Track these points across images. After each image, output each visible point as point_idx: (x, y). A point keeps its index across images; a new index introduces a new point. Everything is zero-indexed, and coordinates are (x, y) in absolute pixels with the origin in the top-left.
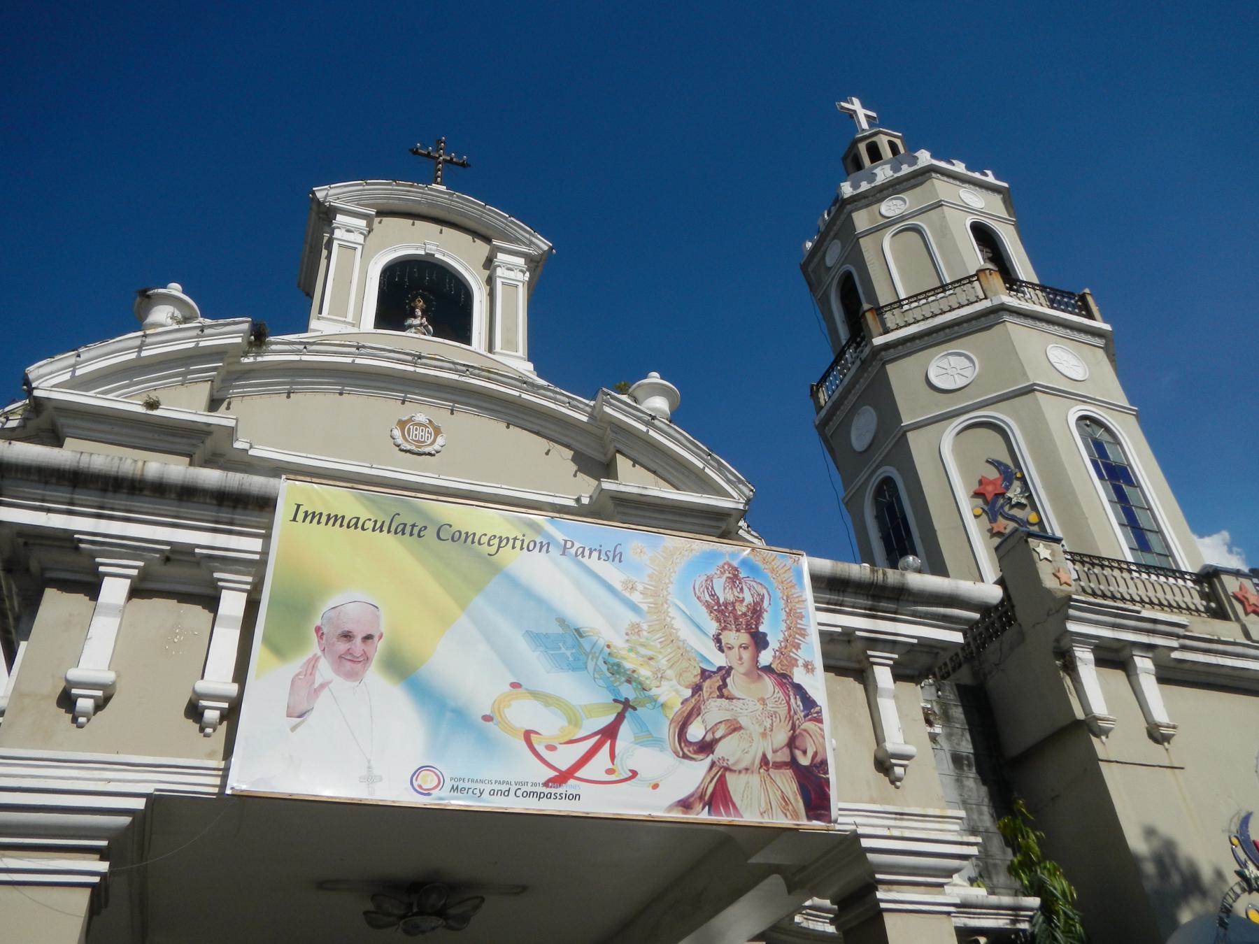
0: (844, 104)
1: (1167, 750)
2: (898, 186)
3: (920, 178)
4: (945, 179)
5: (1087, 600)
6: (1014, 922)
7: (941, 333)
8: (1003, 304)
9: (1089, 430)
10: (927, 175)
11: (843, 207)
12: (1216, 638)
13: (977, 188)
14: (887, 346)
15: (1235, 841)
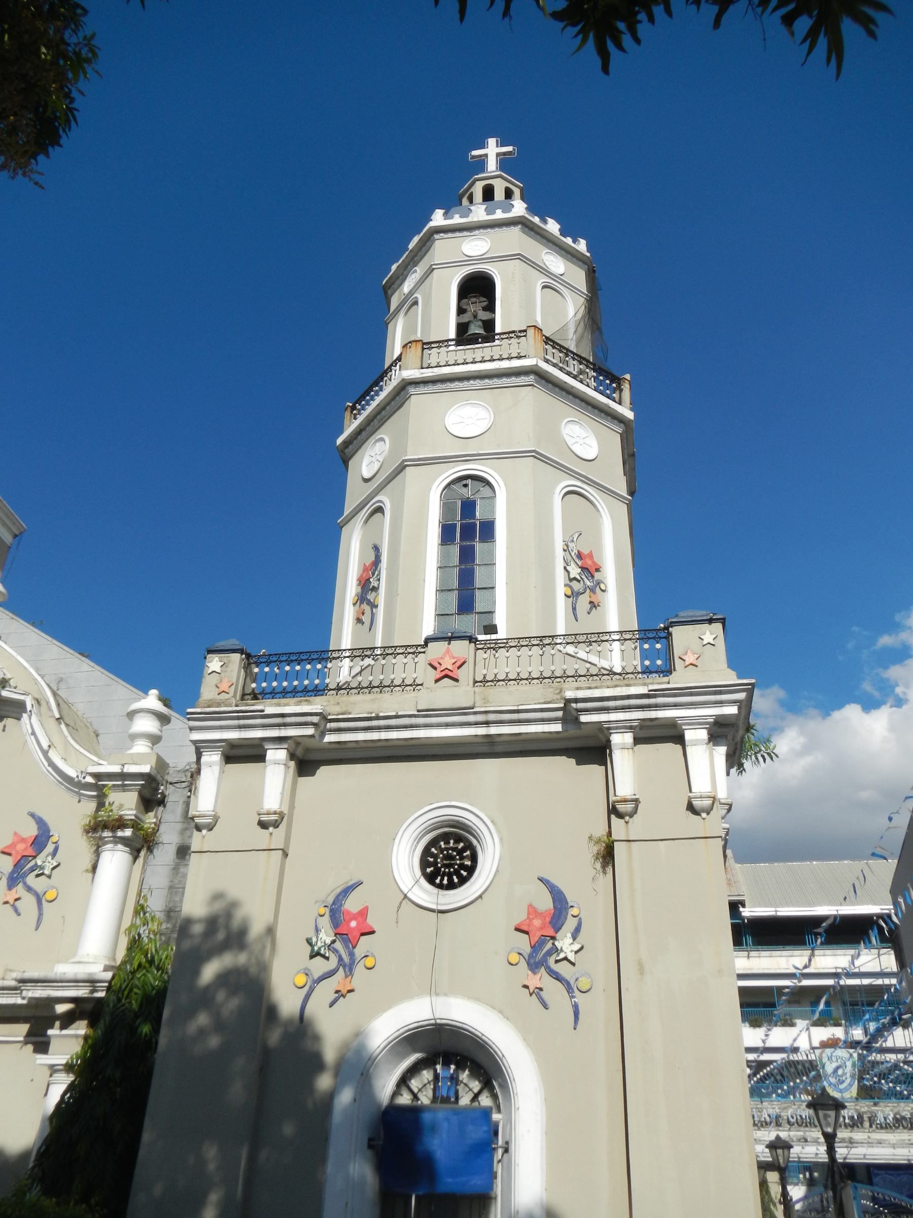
0: (475, 153)
1: (271, 834)
2: (415, 259)
3: (428, 243)
4: (450, 235)
5: (203, 711)
6: (92, 992)
7: (376, 421)
8: (403, 380)
9: (464, 490)
10: (432, 238)
11: (387, 291)
12: (373, 715)
13: (489, 230)
14: (347, 443)
15: (322, 911)
